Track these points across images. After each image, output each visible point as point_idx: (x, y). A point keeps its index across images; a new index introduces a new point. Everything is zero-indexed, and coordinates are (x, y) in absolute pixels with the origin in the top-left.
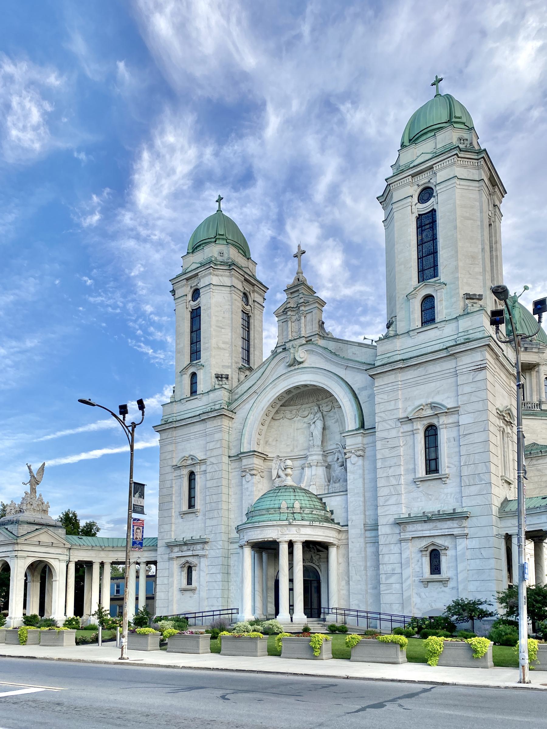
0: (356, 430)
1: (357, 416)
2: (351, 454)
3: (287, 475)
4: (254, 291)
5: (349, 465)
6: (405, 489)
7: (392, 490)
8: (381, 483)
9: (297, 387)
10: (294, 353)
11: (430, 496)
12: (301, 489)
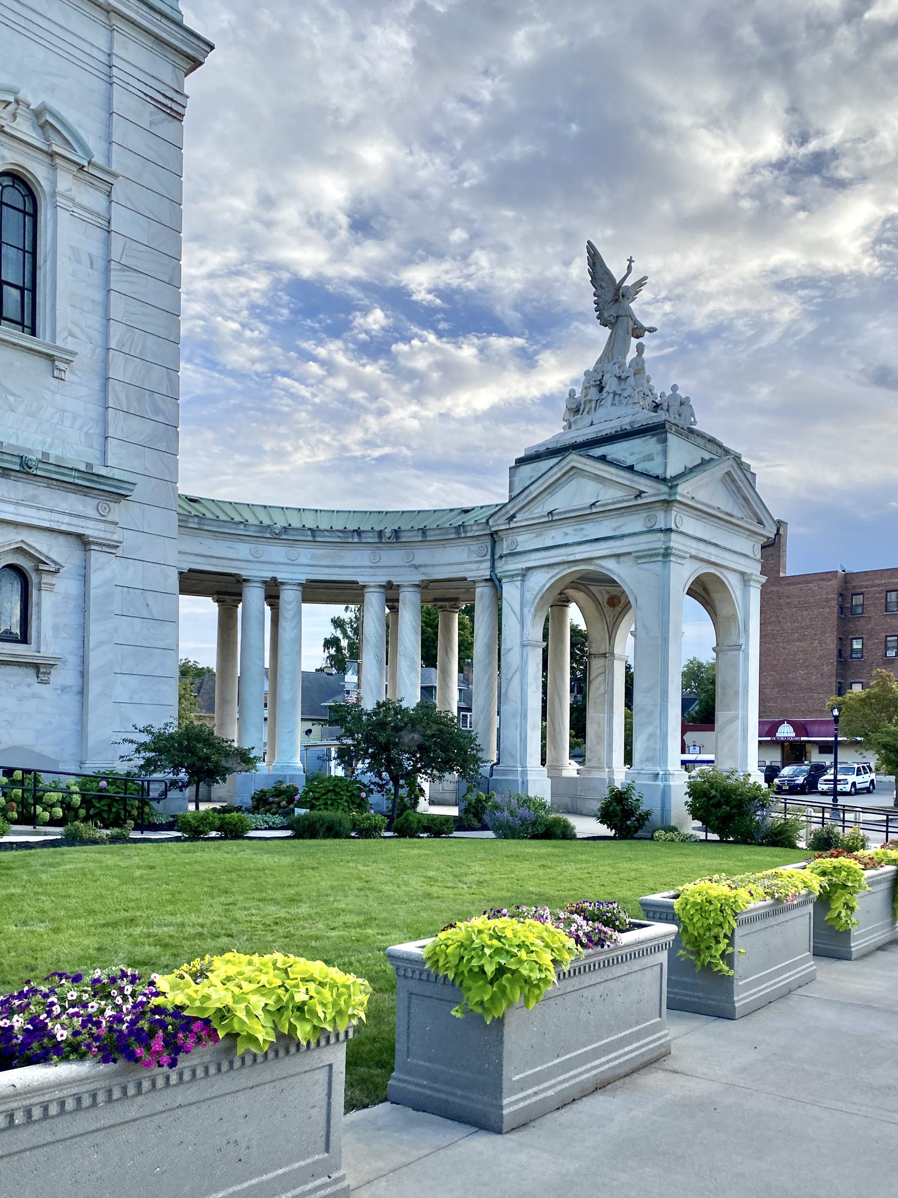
11: (11, 399)
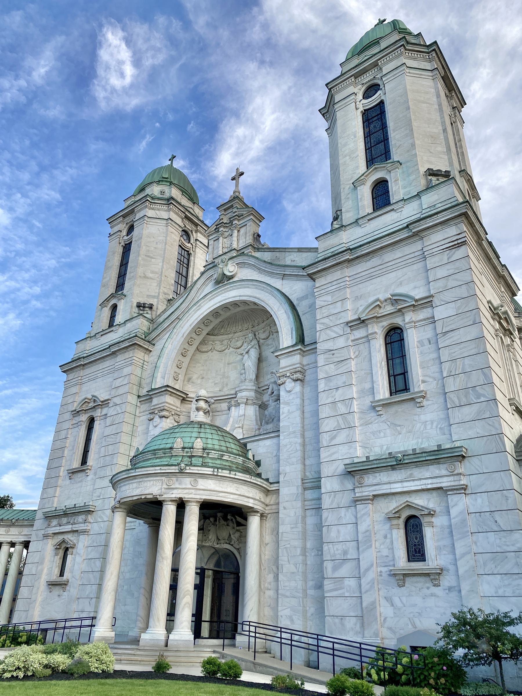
11: (399, 428)
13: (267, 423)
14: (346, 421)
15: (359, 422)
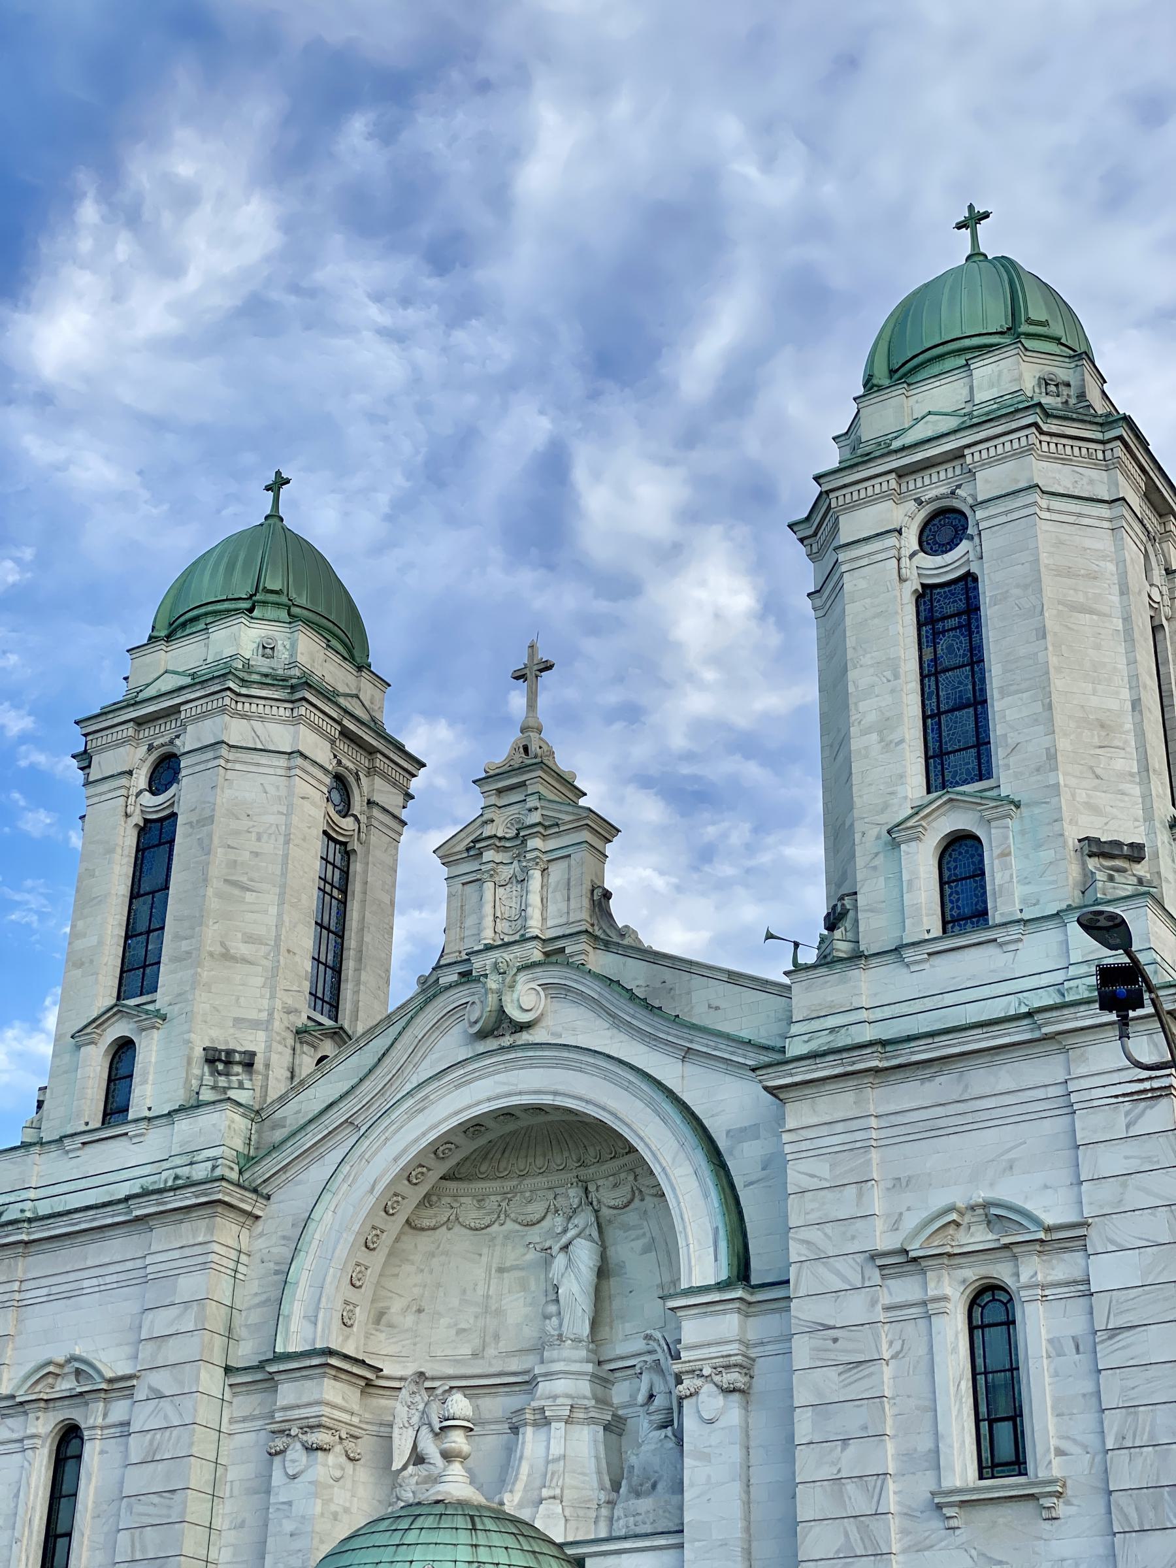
0: (720, 1286)
1: (722, 1233)
2: (699, 1382)
3: (447, 1456)
4: (371, 771)
5: (690, 1424)
6: (904, 1532)
7: (854, 1535)
8: (809, 1504)
9: (507, 1114)
10: (499, 993)
12: (500, 1516)
13: (638, 1495)
14: (869, 1537)
15: (900, 1540)
